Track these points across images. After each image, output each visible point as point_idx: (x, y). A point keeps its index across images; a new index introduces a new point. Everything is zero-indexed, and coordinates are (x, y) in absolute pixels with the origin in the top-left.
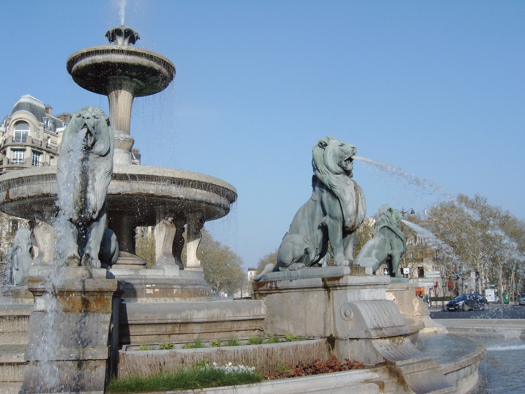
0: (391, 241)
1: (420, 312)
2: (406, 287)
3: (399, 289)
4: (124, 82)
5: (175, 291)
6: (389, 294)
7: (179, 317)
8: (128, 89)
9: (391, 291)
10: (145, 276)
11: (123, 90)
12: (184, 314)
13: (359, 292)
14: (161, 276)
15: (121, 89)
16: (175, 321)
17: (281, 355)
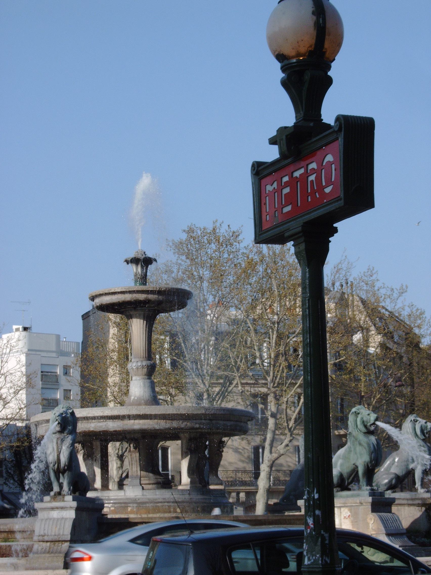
0: (355, 449)
1: (375, 531)
2: (358, 501)
3: (354, 505)
4: (132, 313)
5: (129, 509)
6: (344, 510)
7: (6, 528)
8: (138, 317)
9: (347, 507)
10: (108, 497)
11: (134, 318)
12: (8, 526)
13: (49, 513)
14: (122, 496)
15: (132, 318)
16: (4, 530)
17: (6, 549)
